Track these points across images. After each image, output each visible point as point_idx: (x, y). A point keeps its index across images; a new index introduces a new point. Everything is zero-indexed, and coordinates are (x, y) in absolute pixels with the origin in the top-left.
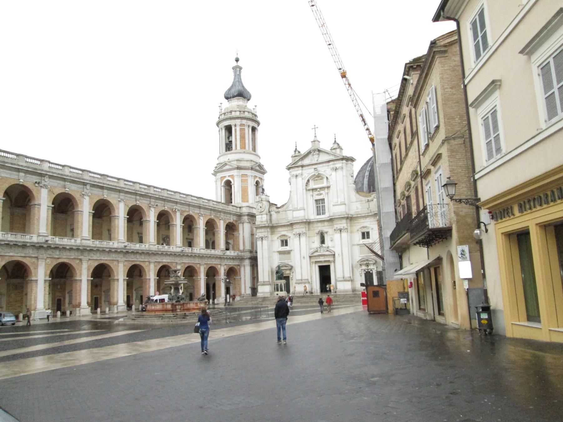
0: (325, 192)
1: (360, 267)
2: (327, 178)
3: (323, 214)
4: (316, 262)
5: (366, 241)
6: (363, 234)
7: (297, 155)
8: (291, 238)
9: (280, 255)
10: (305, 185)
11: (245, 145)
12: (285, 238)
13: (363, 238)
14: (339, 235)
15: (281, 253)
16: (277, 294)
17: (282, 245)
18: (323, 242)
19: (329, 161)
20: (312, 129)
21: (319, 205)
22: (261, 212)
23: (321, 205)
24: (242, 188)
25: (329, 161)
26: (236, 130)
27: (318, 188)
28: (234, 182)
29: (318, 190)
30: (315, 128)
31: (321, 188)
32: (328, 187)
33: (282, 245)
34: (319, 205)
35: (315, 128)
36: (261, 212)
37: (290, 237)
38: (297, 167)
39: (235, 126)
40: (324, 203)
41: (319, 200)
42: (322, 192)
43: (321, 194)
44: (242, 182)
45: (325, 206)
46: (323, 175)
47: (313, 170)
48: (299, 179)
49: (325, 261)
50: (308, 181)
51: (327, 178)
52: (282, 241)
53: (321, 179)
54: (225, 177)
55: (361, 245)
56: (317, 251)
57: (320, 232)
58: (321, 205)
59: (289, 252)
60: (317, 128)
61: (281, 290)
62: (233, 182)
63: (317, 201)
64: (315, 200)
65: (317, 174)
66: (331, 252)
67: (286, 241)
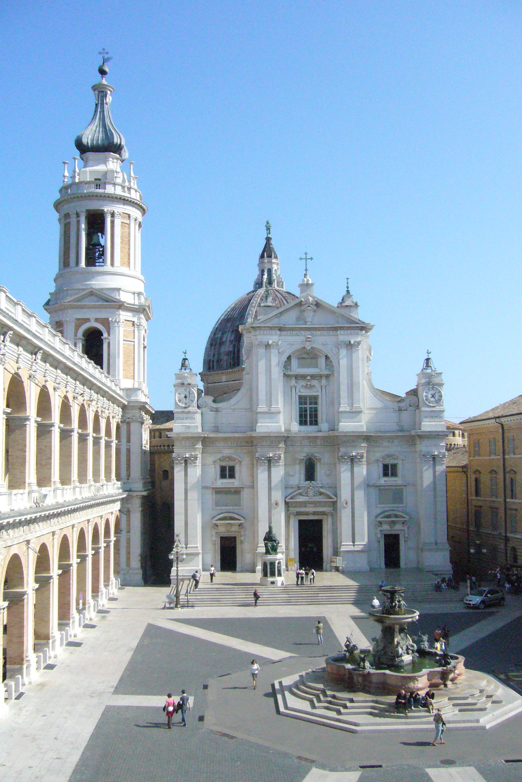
0: (320, 382)
1: (379, 526)
2: (327, 357)
3: (311, 424)
4: (298, 514)
5: (390, 480)
6: (386, 467)
7: (271, 304)
8: (243, 463)
9: (219, 496)
10: (282, 364)
11: (129, 259)
12: (231, 464)
13: (386, 474)
14: (349, 466)
15: (218, 491)
16: (273, 583)
17: (223, 476)
18: (310, 475)
19: (336, 329)
20: (301, 259)
21: (306, 406)
22: (185, 408)
23: (308, 406)
24: (124, 347)
25: (336, 329)
26: (113, 222)
27: (308, 375)
28: (109, 335)
29: (309, 378)
30: (306, 259)
31: (313, 377)
32: (327, 376)
33: (223, 476)
34: (306, 406)
35: (306, 259)
36: (185, 408)
37: (240, 462)
38: (271, 328)
39: (113, 215)
40: (316, 403)
41: (305, 397)
42: (315, 382)
43: (312, 387)
44: (124, 336)
45: (316, 410)
46: (320, 351)
47: (305, 339)
48: (274, 352)
49: (314, 513)
50: (289, 358)
51: (327, 357)
52: (223, 469)
53: (312, 358)
54: (88, 320)
55: (382, 488)
56: (301, 494)
57: (307, 457)
58: (308, 406)
59: (237, 491)
60: (311, 259)
61: (280, 575)
62: (105, 335)
63: (302, 400)
64: (299, 396)
65: (309, 348)
66: (331, 498)
67: (232, 469)
